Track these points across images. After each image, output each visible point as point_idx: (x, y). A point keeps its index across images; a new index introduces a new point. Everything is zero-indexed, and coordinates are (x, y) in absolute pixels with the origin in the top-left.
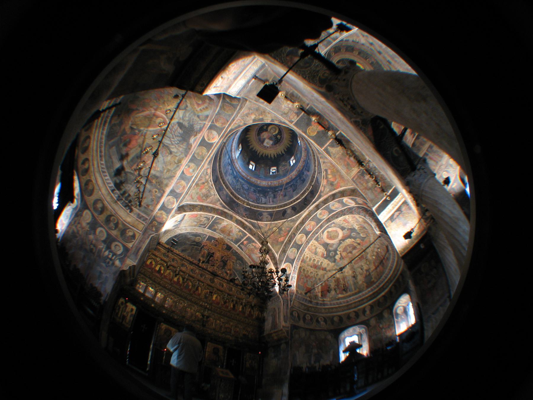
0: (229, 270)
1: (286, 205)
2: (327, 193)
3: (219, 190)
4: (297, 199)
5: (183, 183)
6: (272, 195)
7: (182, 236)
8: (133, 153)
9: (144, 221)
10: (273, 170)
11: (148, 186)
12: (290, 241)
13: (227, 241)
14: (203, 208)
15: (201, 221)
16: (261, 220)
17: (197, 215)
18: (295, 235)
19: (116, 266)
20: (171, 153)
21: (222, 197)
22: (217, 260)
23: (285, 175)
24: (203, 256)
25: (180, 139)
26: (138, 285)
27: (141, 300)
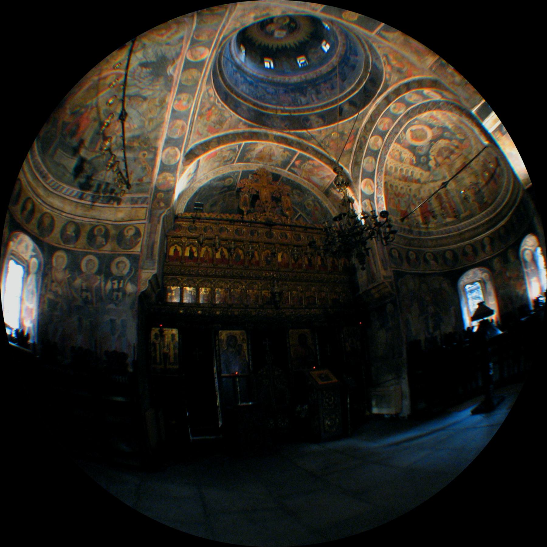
5: (180, 123)
11: (129, 155)
13: (270, 168)
14: (220, 141)
15: (224, 158)
16: (311, 127)
17: (215, 153)
19: (130, 294)
24: (245, 205)
26: (169, 294)
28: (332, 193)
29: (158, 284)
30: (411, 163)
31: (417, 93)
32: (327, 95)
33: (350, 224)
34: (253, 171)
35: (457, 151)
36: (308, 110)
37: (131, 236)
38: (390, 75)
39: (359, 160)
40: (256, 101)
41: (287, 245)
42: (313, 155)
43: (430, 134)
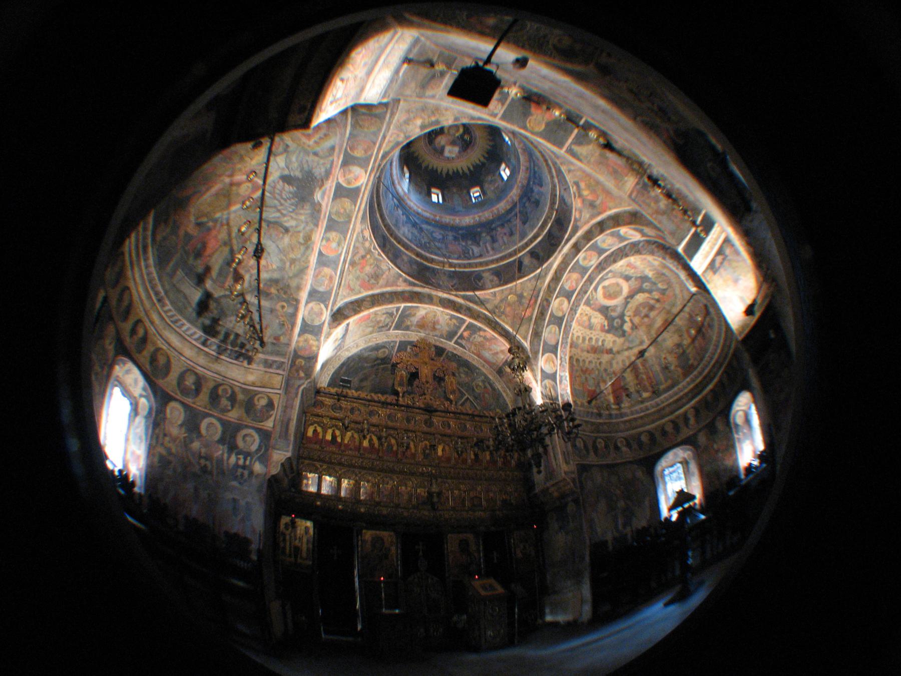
1: (520, 250)
3: (395, 257)
9: (278, 368)
12: (542, 314)
13: (433, 340)
14: (375, 300)
15: (378, 322)
17: (369, 315)
18: (549, 303)
20: (287, 230)
21: (402, 267)
26: (305, 481)
27: (317, 507)
29: (292, 468)
30: (603, 329)
31: (612, 235)
32: (505, 244)
33: (526, 421)
35: (658, 305)
37: (263, 406)
38: (581, 212)
40: (419, 250)
41: (450, 436)
42: (484, 324)
43: (626, 288)
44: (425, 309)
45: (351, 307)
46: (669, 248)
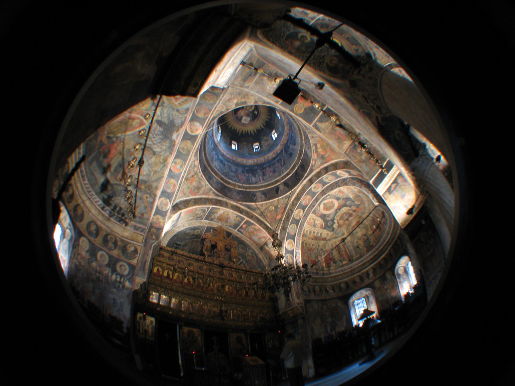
0: (234, 258)
2: (319, 167)
3: (209, 179)
4: (288, 174)
6: (261, 173)
7: (181, 234)
8: (115, 163)
9: (142, 231)
10: (256, 146)
12: (288, 218)
14: (197, 202)
15: (197, 214)
16: (255, 201)
17: (192, 210)
18: (292, 212)
22: (221, 251)
23: (269, 151)
25: (161, 137)
26: (151, 296)
28: (265, 249)
30: (321, 227)
34: (214, 228)
35: (354, 214)
36: (256, 188)
37: (131, 252)
39: (286, 226)
42: (255, 221)
43: (336, 204)
44: (223, 210)
45: (183, 203)
46: (364, 181)
